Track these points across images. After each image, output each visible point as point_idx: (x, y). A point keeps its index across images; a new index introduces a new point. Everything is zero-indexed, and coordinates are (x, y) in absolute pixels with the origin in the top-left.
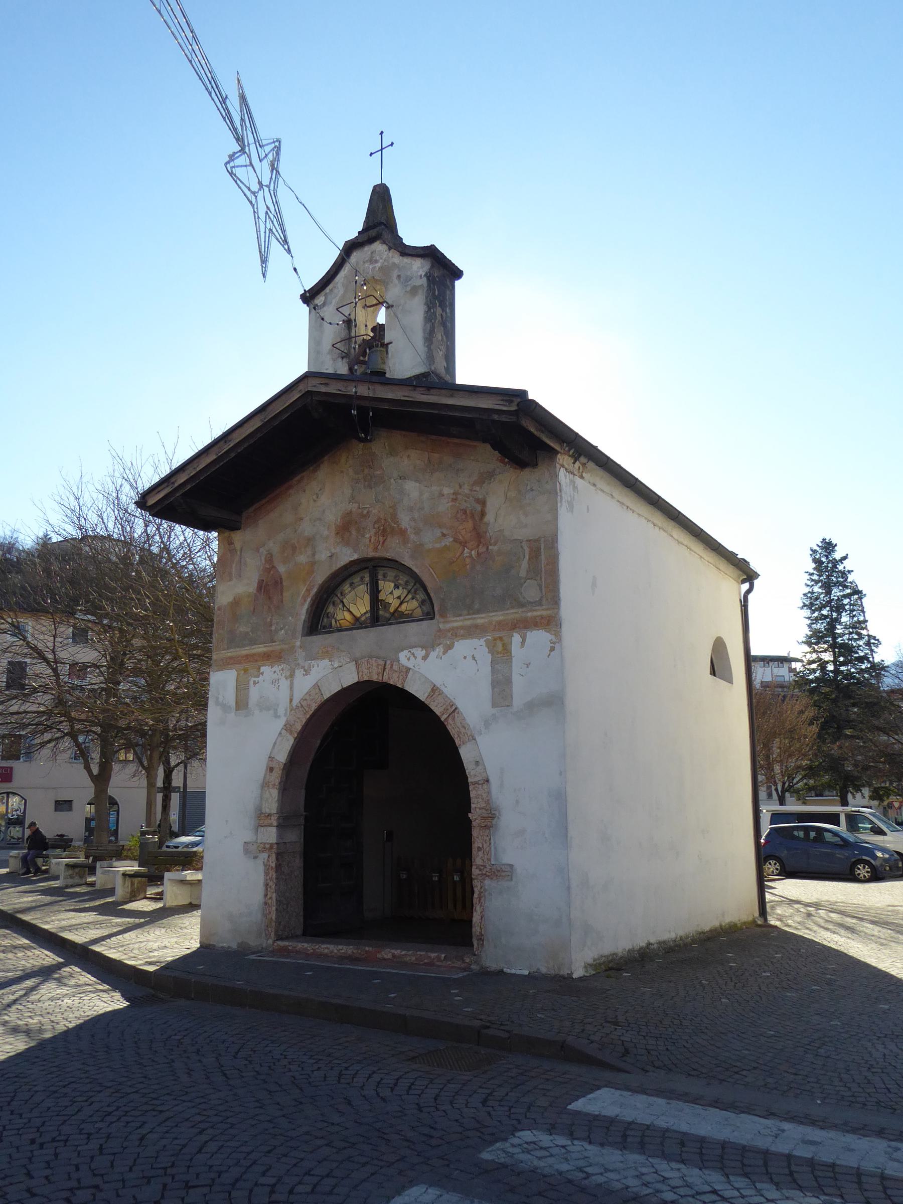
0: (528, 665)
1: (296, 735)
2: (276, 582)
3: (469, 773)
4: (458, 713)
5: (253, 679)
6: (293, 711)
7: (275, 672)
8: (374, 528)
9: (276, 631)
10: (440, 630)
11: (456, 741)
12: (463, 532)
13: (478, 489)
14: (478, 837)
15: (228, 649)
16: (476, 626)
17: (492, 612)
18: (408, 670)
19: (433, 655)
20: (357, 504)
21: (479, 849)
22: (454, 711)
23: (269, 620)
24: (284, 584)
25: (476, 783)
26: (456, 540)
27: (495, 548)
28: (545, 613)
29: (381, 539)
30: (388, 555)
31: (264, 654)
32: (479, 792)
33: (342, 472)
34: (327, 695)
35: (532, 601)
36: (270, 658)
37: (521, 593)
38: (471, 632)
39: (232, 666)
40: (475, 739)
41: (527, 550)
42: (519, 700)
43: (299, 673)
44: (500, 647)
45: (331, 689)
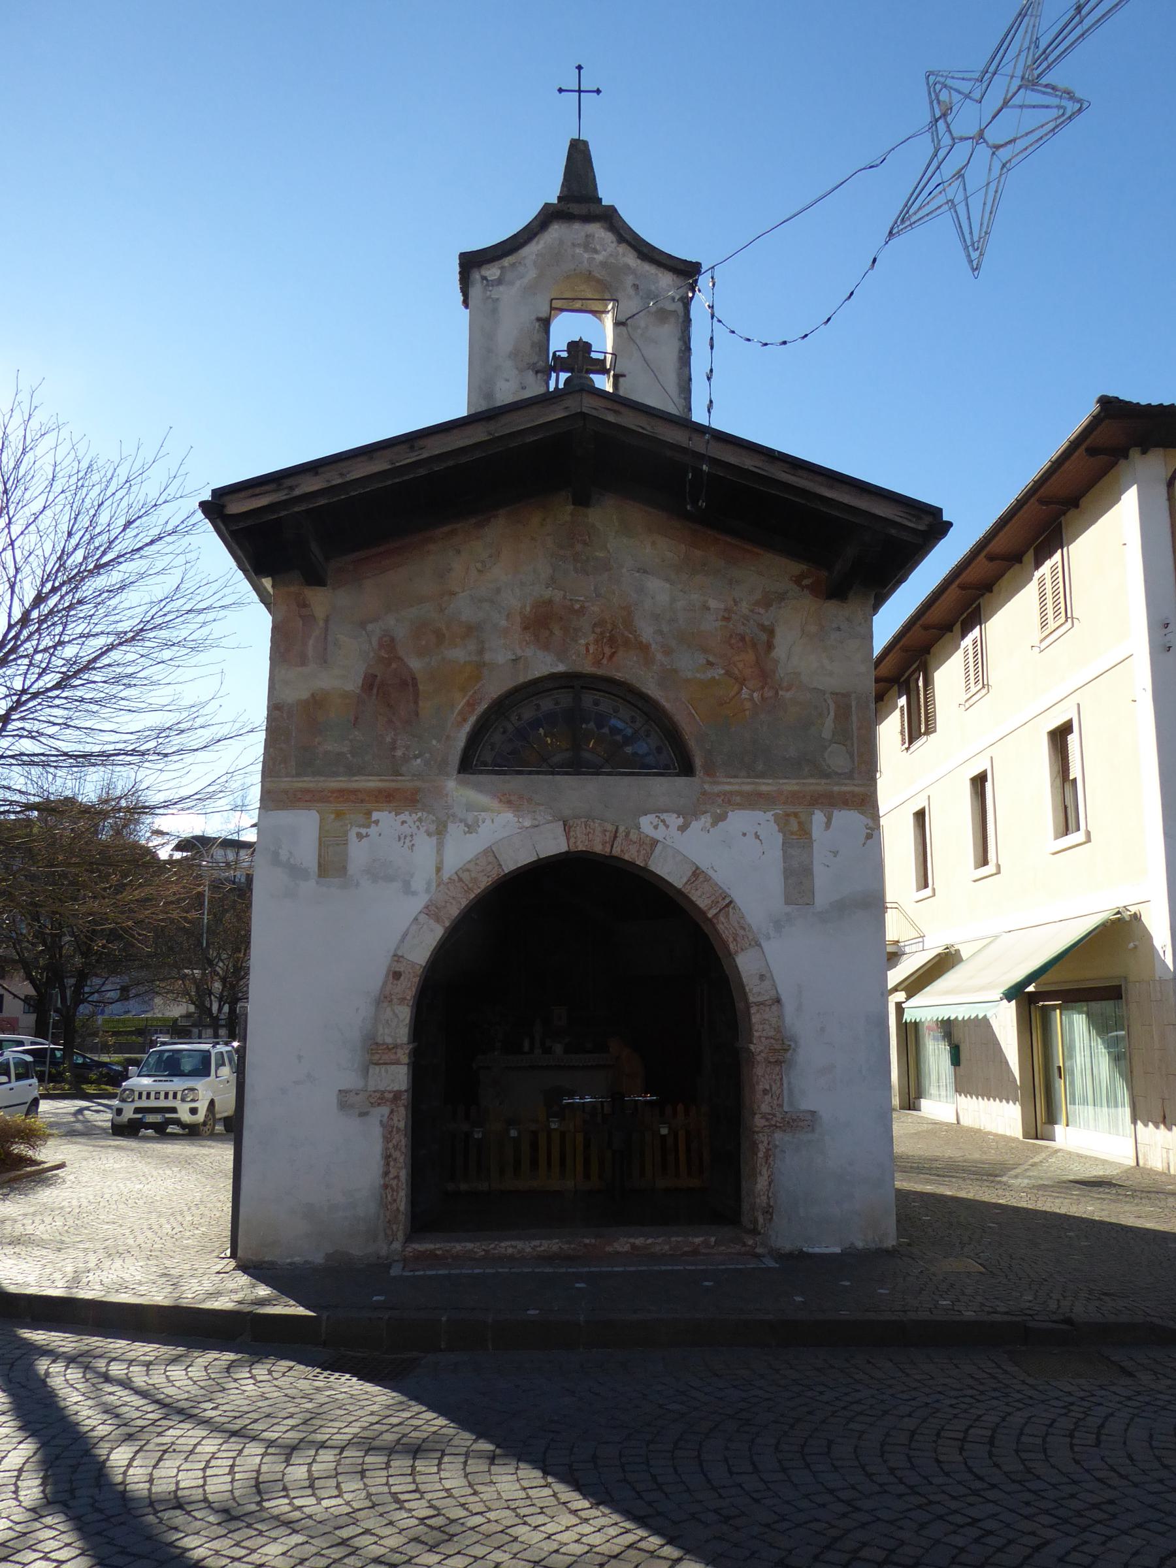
0: (835, 854)
1: (447, 924)
2: (404, 684)
3: (751, 990)
4: (734, 908)
5: (355, 830)
6: (442, 886)
7: (403, 822)
8: (593, 632)
9: (406, 759)
10: (704, 793)
11: (732, 946)
12: (740, 665)
13: (762, 611)
14: (764, 1076)
15: (298, 775)
16: (760, 795)
17: (781, 778)
18: (654, 843)
19: (696, 826)
20: (562, 592)
21: (765, 1092)
22: (728, 905)
23: (388, 739)
24: (421, 687)
25: (762, 1003)
26: (728, 673)
27: (788, 695)
28: (856, 789)
29: (608, 651)
30: (618, 676)
31: (380, 791)
32: (766, 1016)
33: (533, 539)
34: (510, 866)
35: (840, 771)
36: (387, 798)
37: (824, 760)
38: (753, 801)
39: (309, 804)
40: (760, 945)
41: (832, 707)
42: (822, 899)
43: (455, 830)
44: (795, 827)
45: (518, 857)
